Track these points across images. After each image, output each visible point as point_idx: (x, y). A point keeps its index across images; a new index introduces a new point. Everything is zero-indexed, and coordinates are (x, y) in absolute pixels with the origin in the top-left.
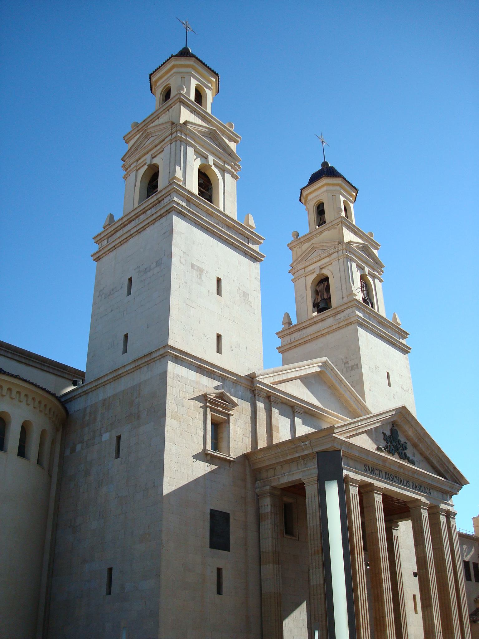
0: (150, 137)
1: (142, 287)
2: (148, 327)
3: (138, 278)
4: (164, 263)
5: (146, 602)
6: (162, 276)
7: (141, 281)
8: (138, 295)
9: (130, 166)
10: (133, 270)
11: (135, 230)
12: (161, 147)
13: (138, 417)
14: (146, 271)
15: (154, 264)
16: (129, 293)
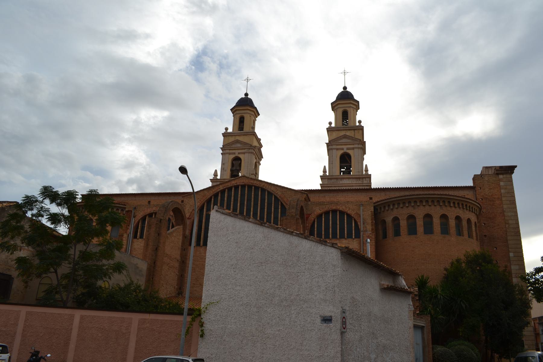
12: (354, 148)
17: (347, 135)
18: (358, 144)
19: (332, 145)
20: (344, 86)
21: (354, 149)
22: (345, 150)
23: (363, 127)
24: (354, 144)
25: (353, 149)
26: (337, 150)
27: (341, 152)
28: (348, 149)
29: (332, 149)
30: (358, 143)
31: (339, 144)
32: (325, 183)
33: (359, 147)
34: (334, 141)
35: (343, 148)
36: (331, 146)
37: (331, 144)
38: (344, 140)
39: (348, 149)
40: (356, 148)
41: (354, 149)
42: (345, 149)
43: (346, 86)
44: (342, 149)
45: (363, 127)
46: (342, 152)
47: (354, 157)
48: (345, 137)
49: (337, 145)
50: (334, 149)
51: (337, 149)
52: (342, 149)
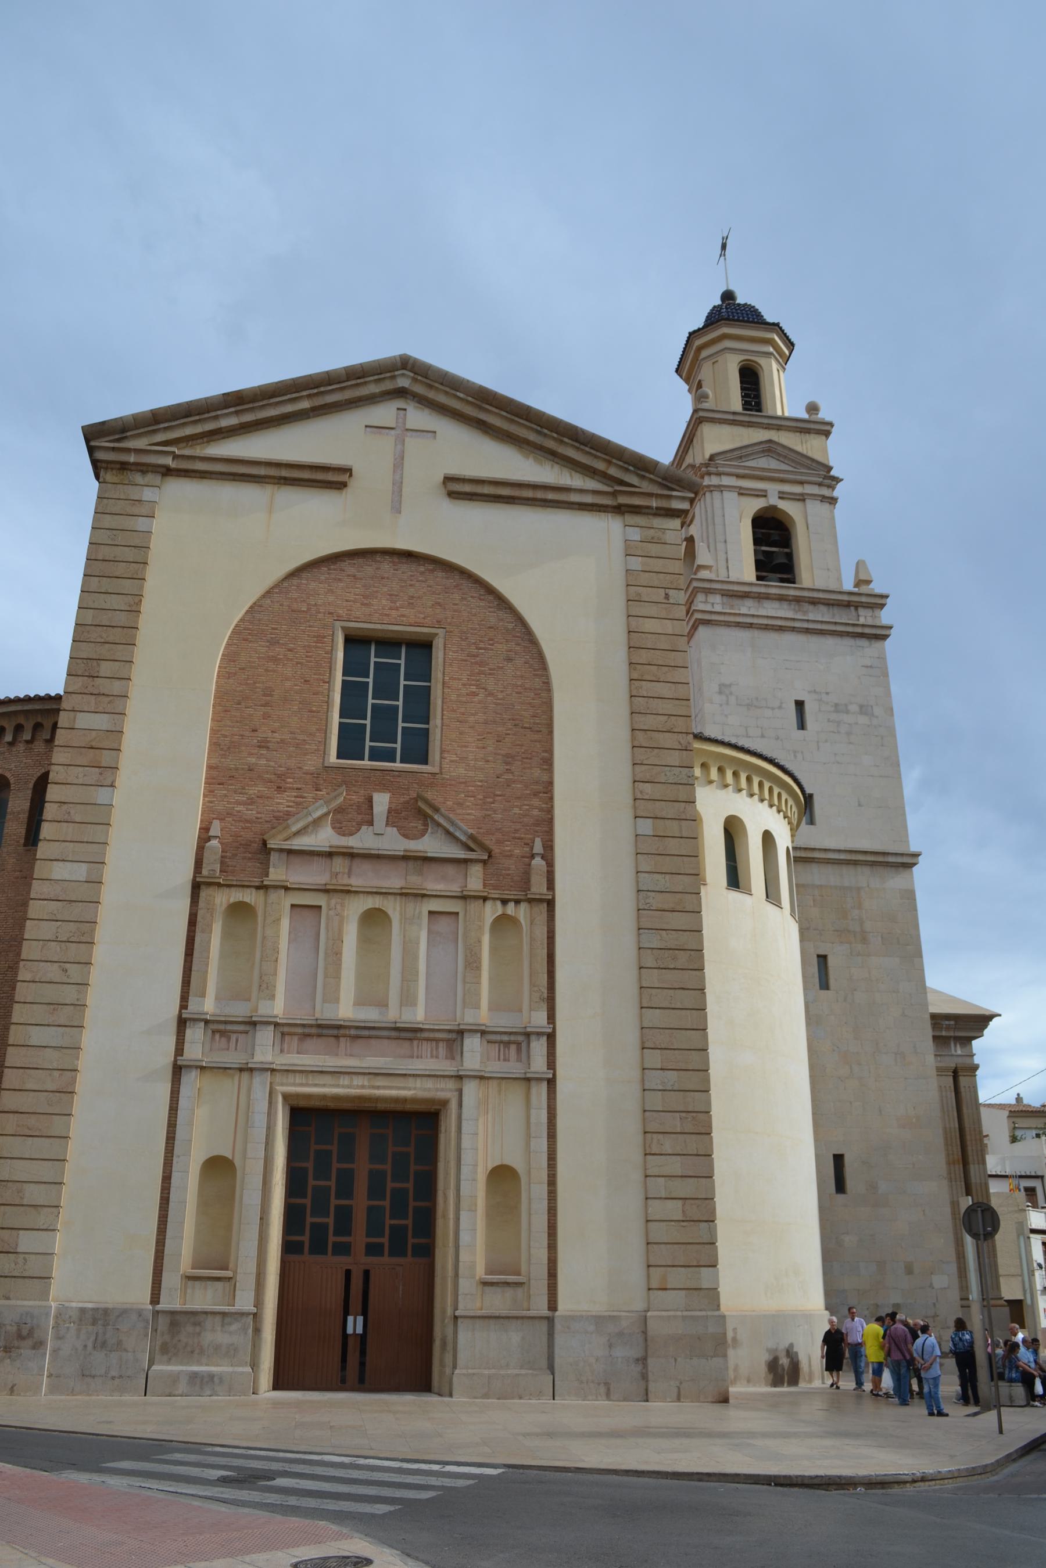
0: (768, 455)
1: (833, 732)
2: (860, 805)
3: (820, 711)
4: (877, 717)
5: (924, 1211)
6: (877, 736)
7: (829, 721)
8: (826, 741)
9: (719, 474)
10: (804, 690)
11: (805, 625)
12: (802, 494)
13: (864, 940)
14: (837, 708)
15: (854, 708)
16: (802, 725)
18: (820, 485)
21: (804, 500)
22: (773, 500)
23: (831, 424)
24: (802, 483)
25: (801, 498)
26: (740, 494)
27: (756, 505)
28: (782, 496)
29: (719, 486)
30: (821, 480)
31: (747, 472)
33: (824, 497)
34: (730, 460)
35: (766, 491)
36: (713, 477)
37: (715, 469)
40: (814, 496)
41: (804, 500)
44: (763, 494)
47: (808, 529)
48: (770, 449)
49: (738, 476)
51: (742, 492)
52: (763, 494)
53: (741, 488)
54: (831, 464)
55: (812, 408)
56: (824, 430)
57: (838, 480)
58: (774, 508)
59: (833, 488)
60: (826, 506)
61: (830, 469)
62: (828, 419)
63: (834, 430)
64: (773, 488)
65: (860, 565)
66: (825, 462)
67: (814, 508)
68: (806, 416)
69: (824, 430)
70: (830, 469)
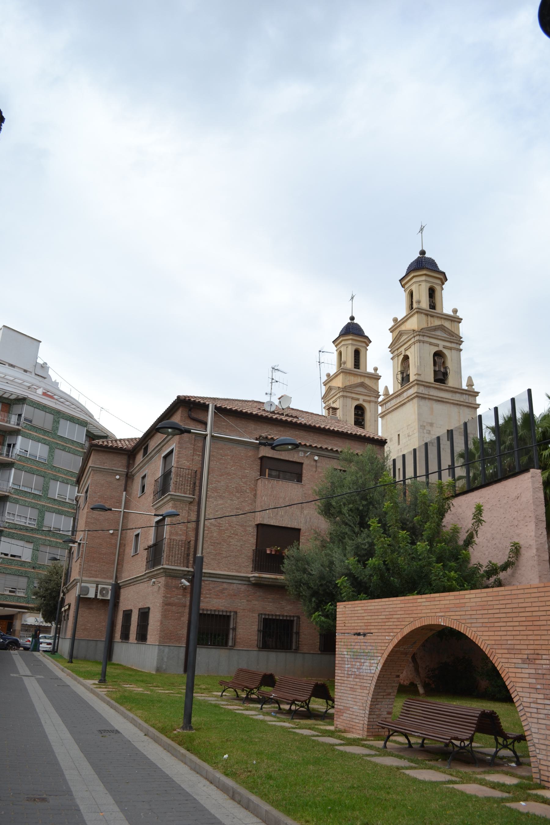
17: (445, 327)
19: (424, 336)
20: (421, 249)
21: (451, 349)
22: (441, 348)
23: (462, 319)
24: (451, 342)
25: (451, 349)
31: (433, 336)
32: (420, 391)
34: (427, 331)
38: (439, 333)
39: (445, 347)
41: (451, 349)
42: (441, 345)
43: (424, 249)
44: (437, 345)
45: (462, 319)
46: (435, 349)
49: (429, 337)
50: (427, 342)
51: (431, 344)
52: (437, 345)
53: (431, 342)
54: (461, 335)
55: (455, 311)
56: (459, 320)
57: (462, 342)
58: (441, 351)
59: (460, 344)
60: (458, 352)
61: (461, 338)
62: (460, 317)
63: (462, 321)
64: (441, 343)
65: (470, 379)
66: (458, 334)
67: (454, 352)
68: (452, 314)
69: (459, 320)
70: (461, 338)
